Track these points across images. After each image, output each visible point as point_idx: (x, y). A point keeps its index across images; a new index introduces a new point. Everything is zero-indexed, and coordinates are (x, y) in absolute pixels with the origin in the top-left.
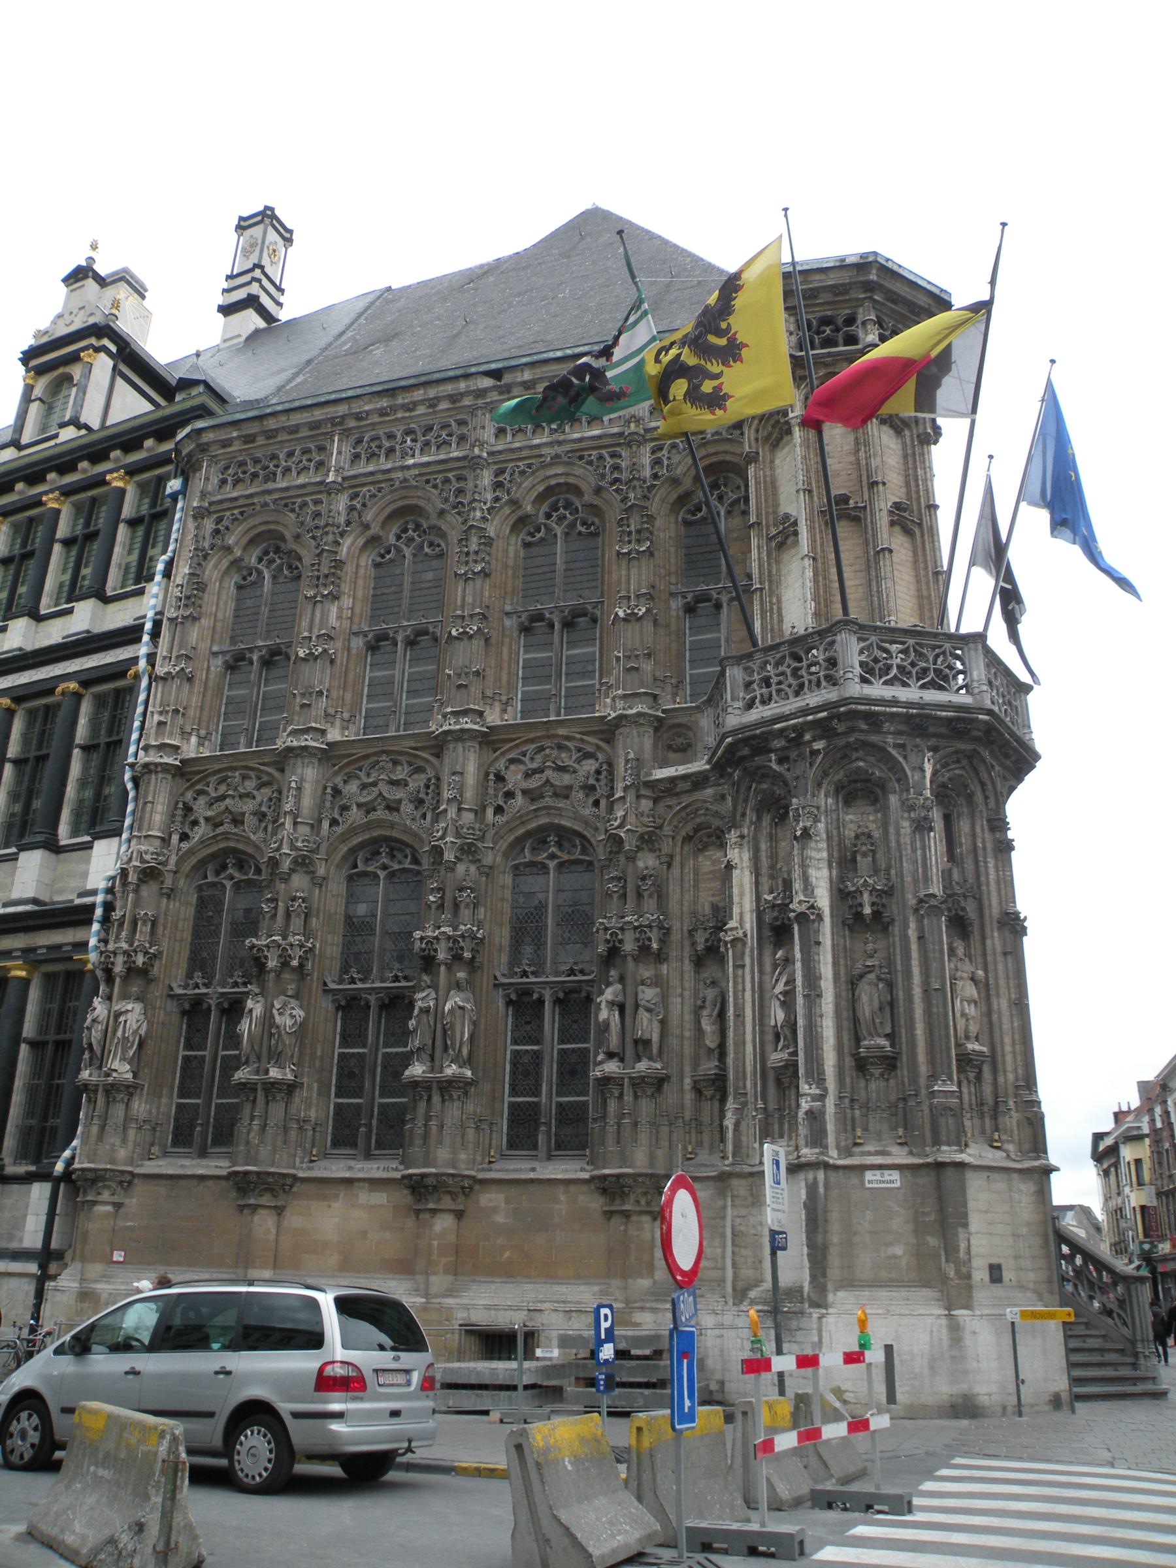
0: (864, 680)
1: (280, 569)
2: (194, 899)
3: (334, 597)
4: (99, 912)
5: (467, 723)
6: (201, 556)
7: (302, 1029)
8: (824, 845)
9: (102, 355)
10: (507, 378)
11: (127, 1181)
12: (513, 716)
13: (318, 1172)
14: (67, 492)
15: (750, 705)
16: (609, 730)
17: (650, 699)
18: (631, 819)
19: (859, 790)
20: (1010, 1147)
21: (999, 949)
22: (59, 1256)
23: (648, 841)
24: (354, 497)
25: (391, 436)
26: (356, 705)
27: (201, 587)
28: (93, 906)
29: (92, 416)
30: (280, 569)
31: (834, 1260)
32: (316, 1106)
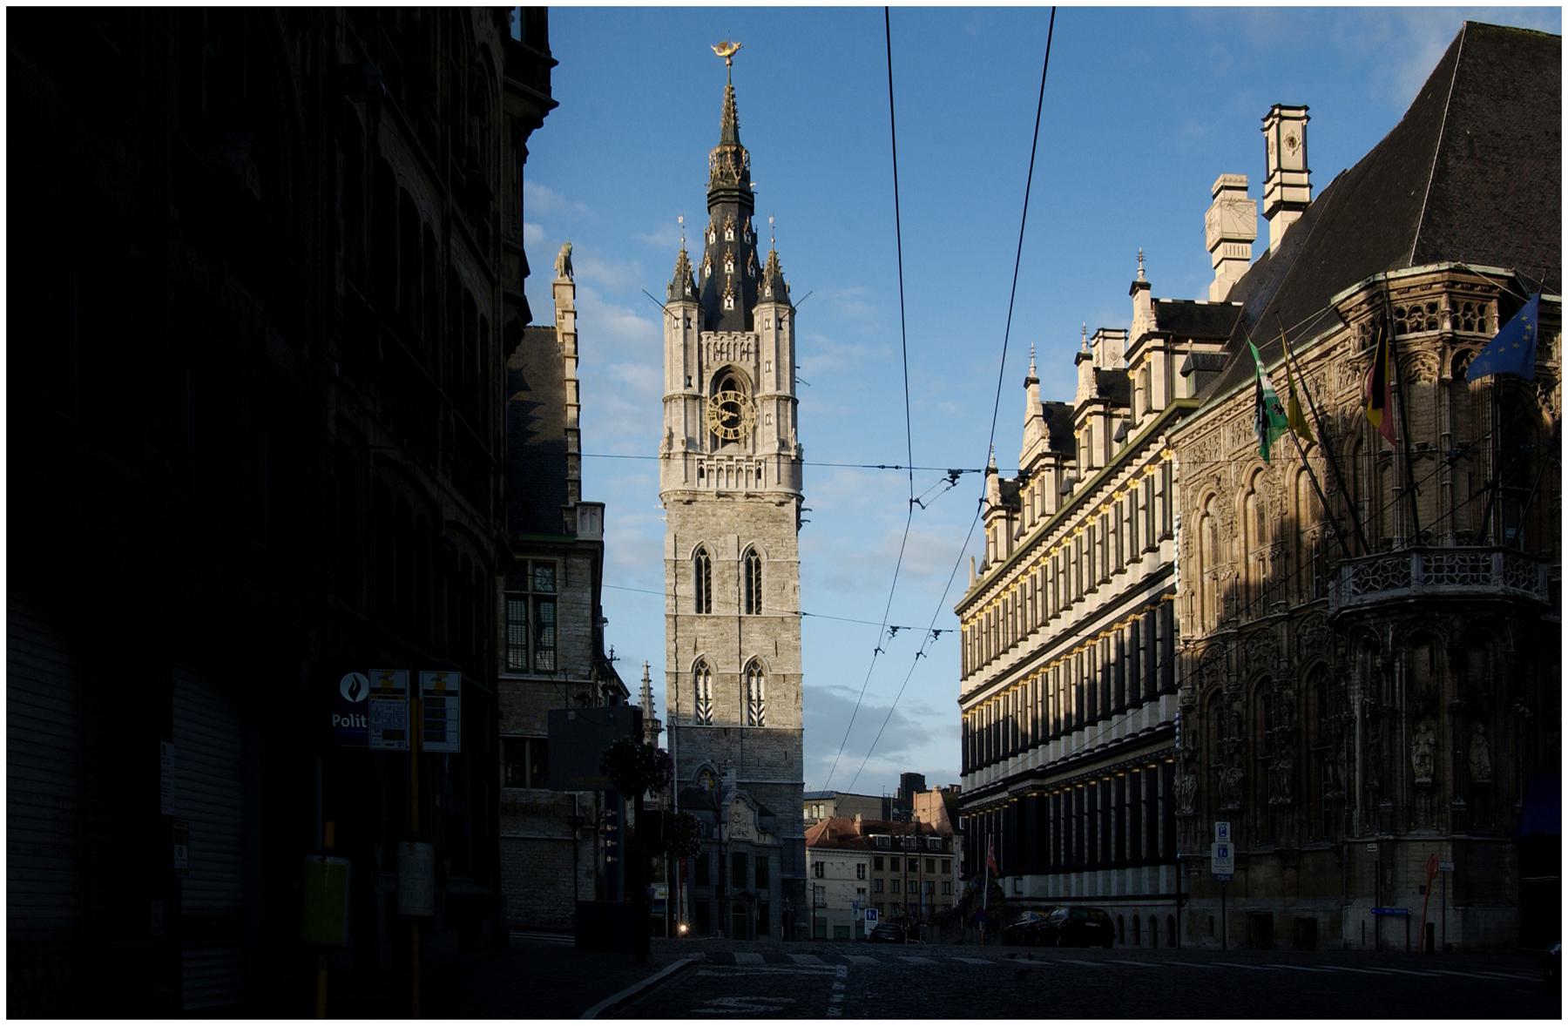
7: (1243, 782)
19: (1373, 647)
22: (1186, 896)
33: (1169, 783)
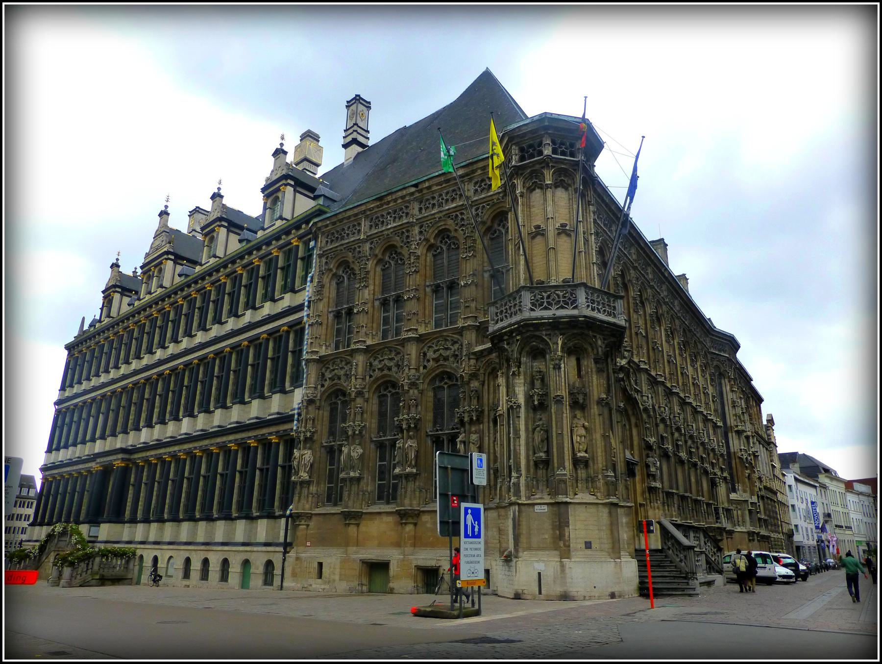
0: (532, 310)
1: (350, 275)
2: (329, 408)
3: (366, 287)
4: (296, 416)
5: (411, 335)
6: (321, 273)
7: (362, 457)
8: (522, 377)
9: (288, 187)
10: (420, 187)
11: (310, 516)
12: (430, 329)
13: (370, 510)
14: (280, 248)
15: (497, 322)
16: (460, 331)
17: (474, 319)
18: (467, 368)
20: (599, 494)
21: (597, 413)
23: (474, 376)
24: (371, 243)
25: (383, 216)
26: (378, 329)
27: (323, 286)
28: (293, 415)
29: (287, 214)
30: (350, 275)
31: (523, 540)
32: (370, 485)
33: (289, 455)
